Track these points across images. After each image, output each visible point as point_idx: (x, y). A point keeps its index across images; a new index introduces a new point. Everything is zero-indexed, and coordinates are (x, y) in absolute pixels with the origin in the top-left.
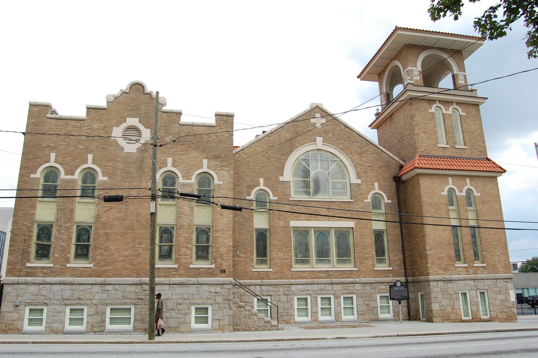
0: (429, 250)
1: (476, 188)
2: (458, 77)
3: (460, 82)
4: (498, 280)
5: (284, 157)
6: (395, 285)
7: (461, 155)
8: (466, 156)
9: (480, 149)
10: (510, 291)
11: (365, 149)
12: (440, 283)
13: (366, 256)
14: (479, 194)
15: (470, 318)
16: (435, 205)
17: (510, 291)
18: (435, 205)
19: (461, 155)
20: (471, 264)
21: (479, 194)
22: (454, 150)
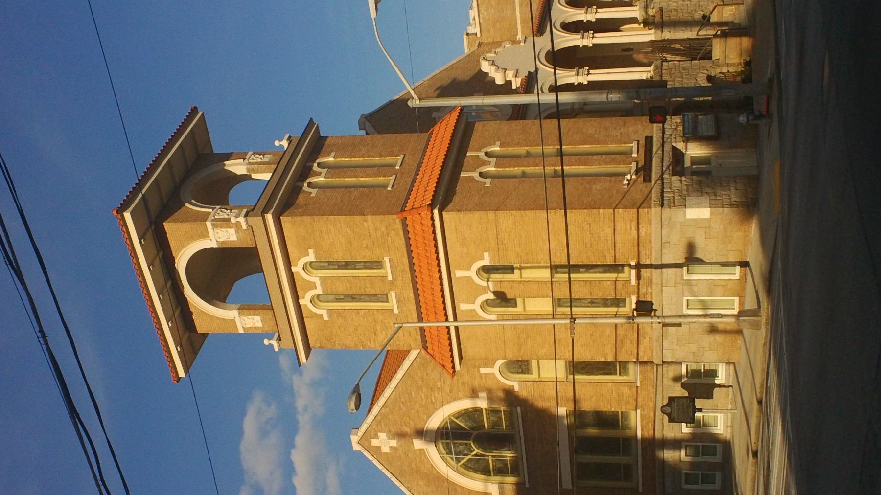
0: (605, 356)
1: (474, 260)
2: (223, 242)
3: (234, 238)
4: (664, 239)
5: (459, 490)
6: (669, 415)
7: (404, 270)
8: (406, 260)
9: (383, 229)
10: (688, 216)
11: (420, 382)
12: (666, 344)
13: (615, 395)
14: (486, 255)
15: (736, 299)
16: (519, 338)
17: (688, 216)
18: (519, 338)
19: (404, 270)
20: (631, 289)
21: (486, 255)
22: (399, 283)
